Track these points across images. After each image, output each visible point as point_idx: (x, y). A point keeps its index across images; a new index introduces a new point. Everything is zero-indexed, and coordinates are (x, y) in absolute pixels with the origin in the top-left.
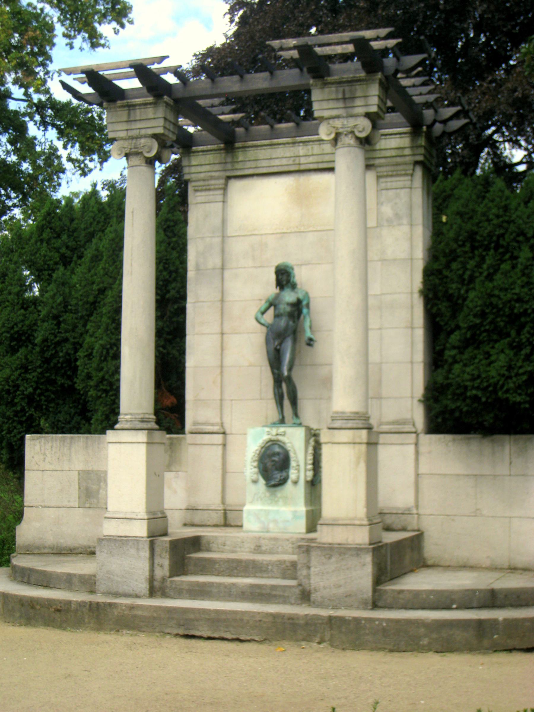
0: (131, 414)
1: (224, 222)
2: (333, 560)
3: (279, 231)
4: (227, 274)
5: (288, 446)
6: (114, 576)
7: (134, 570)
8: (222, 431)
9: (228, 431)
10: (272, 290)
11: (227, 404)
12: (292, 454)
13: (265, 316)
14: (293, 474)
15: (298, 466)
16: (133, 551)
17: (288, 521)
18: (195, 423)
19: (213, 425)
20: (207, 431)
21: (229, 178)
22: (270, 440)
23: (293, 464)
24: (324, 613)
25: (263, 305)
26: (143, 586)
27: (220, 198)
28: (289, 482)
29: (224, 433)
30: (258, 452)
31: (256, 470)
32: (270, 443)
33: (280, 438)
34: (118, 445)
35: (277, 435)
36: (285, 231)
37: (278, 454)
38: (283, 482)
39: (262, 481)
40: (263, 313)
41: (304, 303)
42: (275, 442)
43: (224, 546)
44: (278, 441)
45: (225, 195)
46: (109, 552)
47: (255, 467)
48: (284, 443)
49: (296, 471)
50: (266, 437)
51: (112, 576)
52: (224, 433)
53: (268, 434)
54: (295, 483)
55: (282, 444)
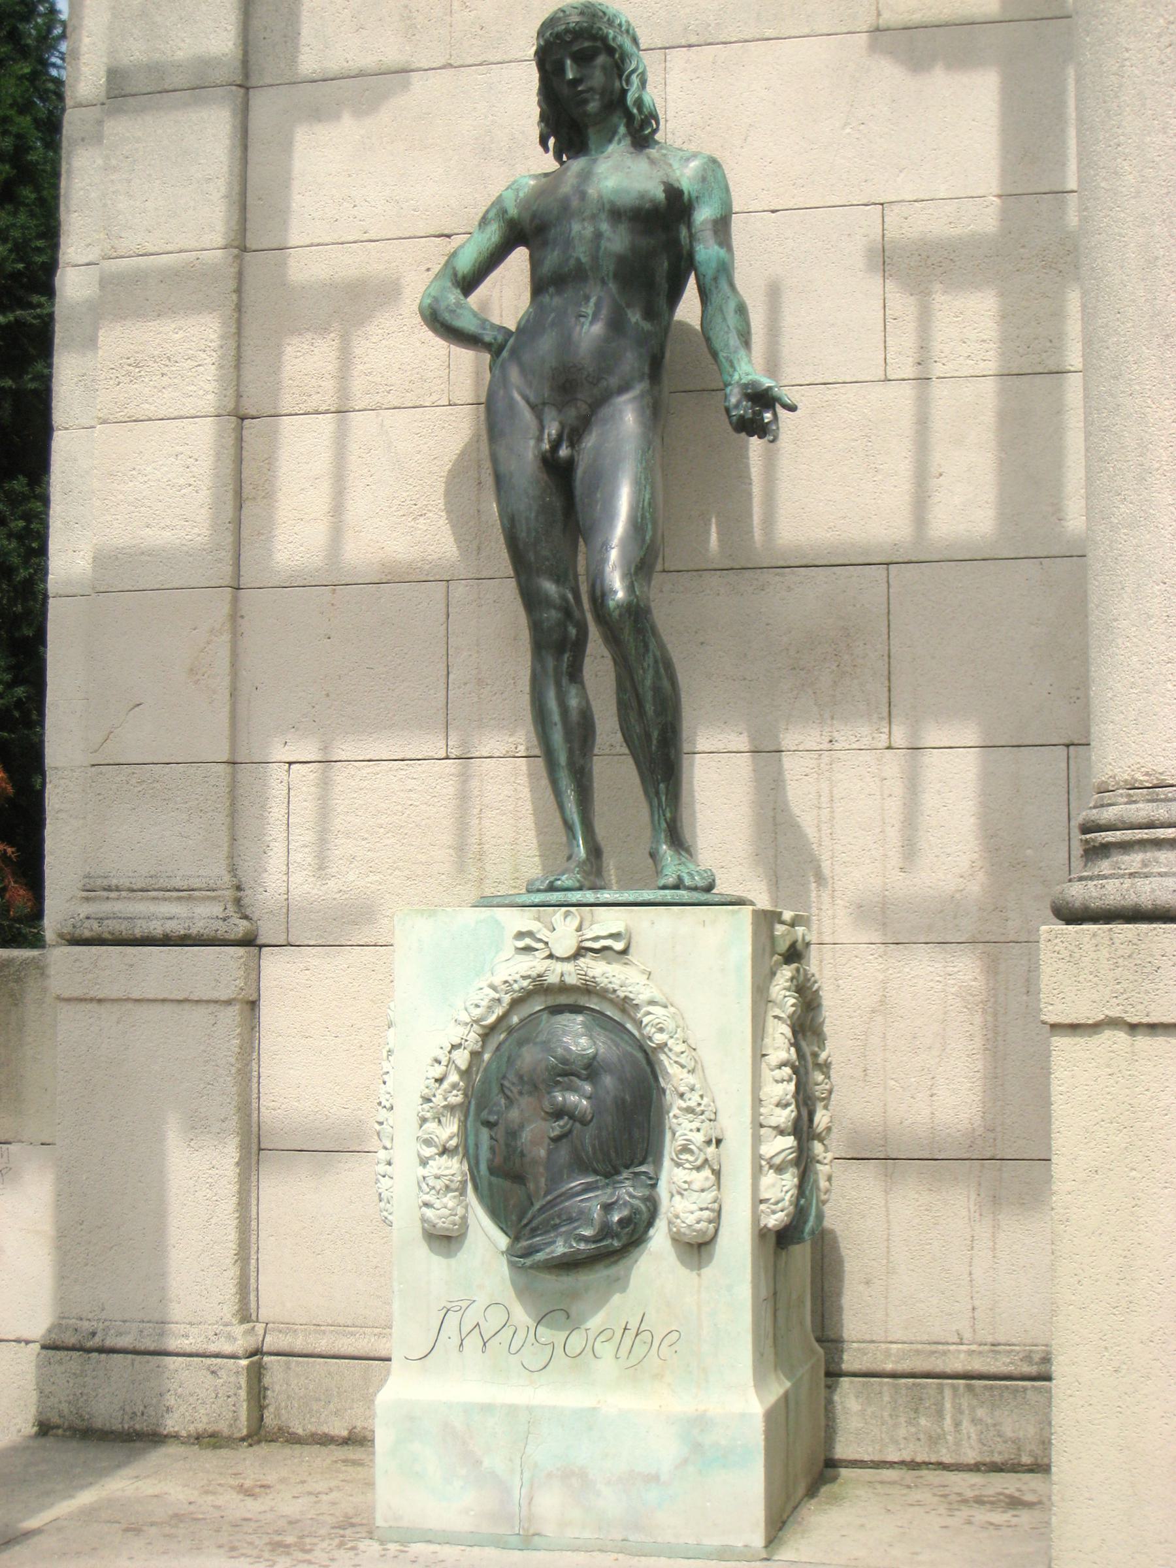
8: (240, 928)
17: (653, 1478)
18: (91, 890)
19: (186, 893)
20: (156, 928)
22: (540, 988)
28: (659, 1239)
30: (462, 1058)
31: (454, 1167)
33: (599, 970)
35: (581, 952)
37: (591, 1069)
41: (704, 215)
42: (563, 1000)
44: (589, 989)
48: (626, 1005)
53: (528, 949)
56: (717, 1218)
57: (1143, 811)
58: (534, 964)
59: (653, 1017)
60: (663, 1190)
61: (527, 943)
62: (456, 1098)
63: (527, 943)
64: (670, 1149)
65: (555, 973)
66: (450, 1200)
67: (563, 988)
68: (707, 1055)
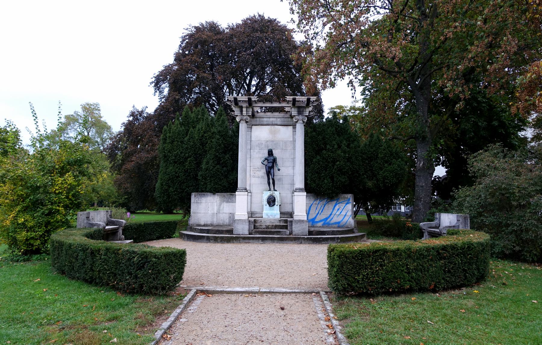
1: (251, 137)
4: (252, 150)
5: (275, 196)
10: (266, 155)
11: (251, 185)
12: (276, 198)
14: (276, 203)
16: (244, 223)
21: (252, 125)
23: (276, 201)
25: (263, 159)
26: (247, 232)
27: (250, 130)
28: (275, 205)
38: (274, 205)
39: (268, 205)
45: (251, 130)
50: (270, 194)
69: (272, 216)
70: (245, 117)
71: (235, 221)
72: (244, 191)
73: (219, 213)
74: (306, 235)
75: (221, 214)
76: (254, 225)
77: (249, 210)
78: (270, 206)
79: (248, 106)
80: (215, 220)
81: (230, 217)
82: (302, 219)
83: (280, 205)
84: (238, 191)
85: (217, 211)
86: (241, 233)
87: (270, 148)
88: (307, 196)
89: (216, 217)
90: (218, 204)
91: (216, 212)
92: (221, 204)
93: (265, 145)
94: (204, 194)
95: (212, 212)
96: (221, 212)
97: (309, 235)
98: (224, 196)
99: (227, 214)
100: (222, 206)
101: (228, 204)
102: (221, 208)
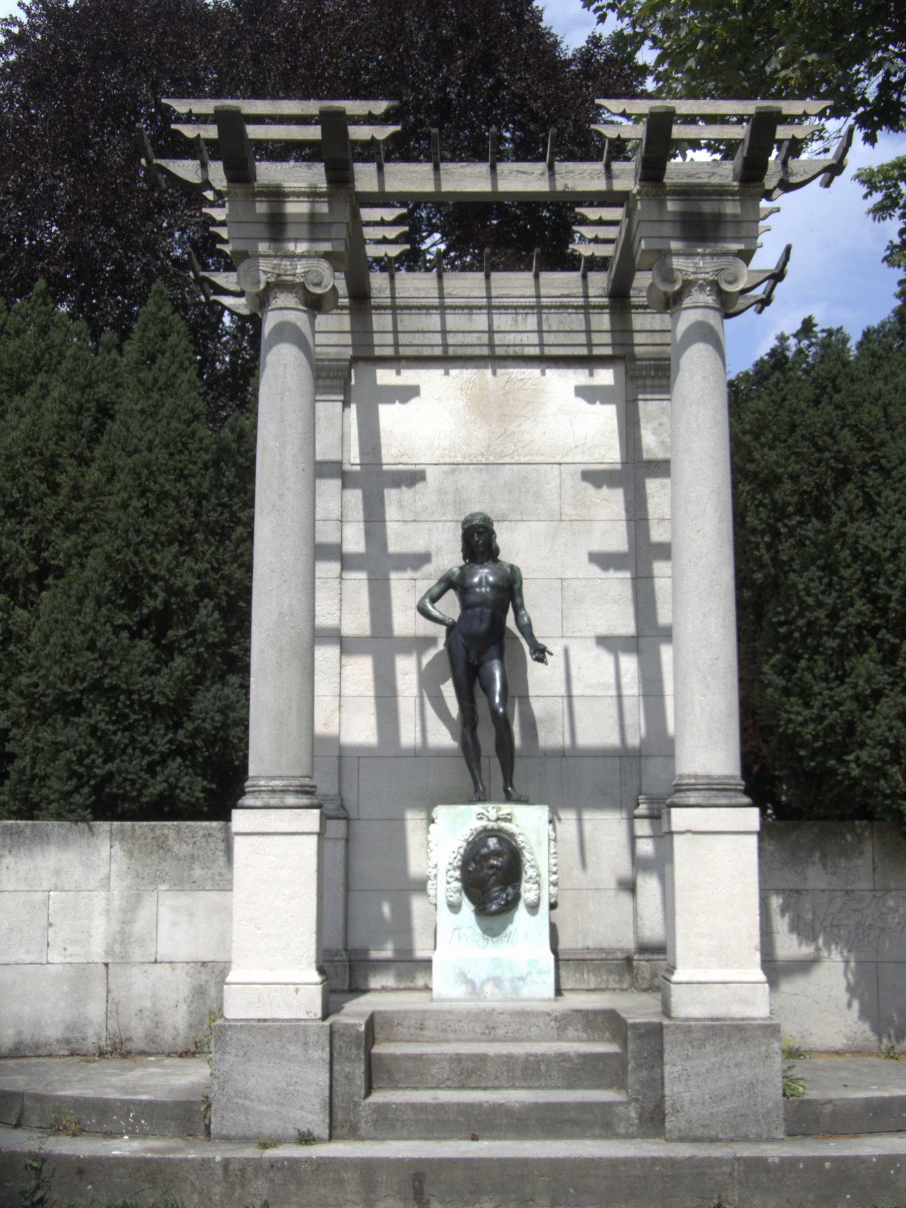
0: (281, 777)
2: (709, 1048)
3: (448, 460)
6: (252, 1100)
7: (297, 1087)
8: (342, 813)
9: (353, 814)
12: (527, 855)
13: (436, 605)
14: (528, 891)
15: (538, 875)
16: (294, 1050)
23: (529, 872)
24: (684, 1151)
28: (521, 906)
29: (347, 819)
30: (462, 851)
31: (458, 885)
32: (483, 835)
34: (257, 838)
35: (498, 819)
36: (459, 459)
38: (511, 905)
39: (468, 907)
40: (434, 600)
43: (421, 1029)
44: (500, 830)
46: (241, 1053)
47: (457, 879)
48: (512, 835)
49: (536, 886)
50: (479, 824)
51: (248, 1103)
52: (347, 819)
53: (481, 819)
54: (533, 908)
55: (507, 837)
56: (539, 899)
57: (693, 781)
58: (484, 823)
59: (520, 839)
60: (522, 890)
61: (480, 817)
62: (460, 863)
63: (480, 817)
64: (525, 877)
65: (491, 825)
66: (458, 895)
67: (493, 830)
68: (535, 850)
69: (497, 981)
70: (301, 267)
71: (223, 1030)
72: (291, 800)
73: (125, 961)
74: (771, 1140)
75: (135, 970)
76: (369, 1060)
77: (336, 943)
78: (481, 910)
79: (323, 186)
80: (95, 1010)
81: (200, 992)
82: (737, 1011)
83: (553, 906)
84: (247, 800)
85: (109, 952)
86: (270, 1127)
87: (476, 507)
88: (765, 834)
89: (99, 989)
90: (116, 903)
91: (97, 951)
92: (138, 898)
93: (441, 491)
94: (21, 832)
95: (75, 953)
96: (137, 955)
97: (791, 1134)
98: (162, 845)
99: (181, 972)
100: (145, 913)
101: (185, 900)
102: (139, 927)
